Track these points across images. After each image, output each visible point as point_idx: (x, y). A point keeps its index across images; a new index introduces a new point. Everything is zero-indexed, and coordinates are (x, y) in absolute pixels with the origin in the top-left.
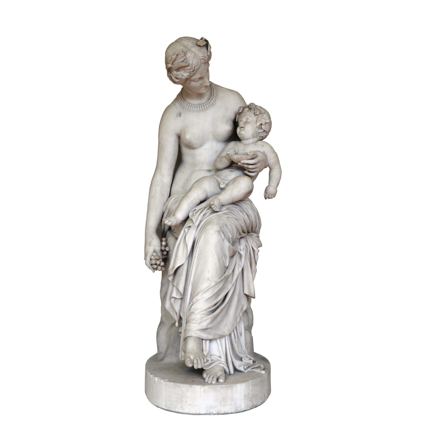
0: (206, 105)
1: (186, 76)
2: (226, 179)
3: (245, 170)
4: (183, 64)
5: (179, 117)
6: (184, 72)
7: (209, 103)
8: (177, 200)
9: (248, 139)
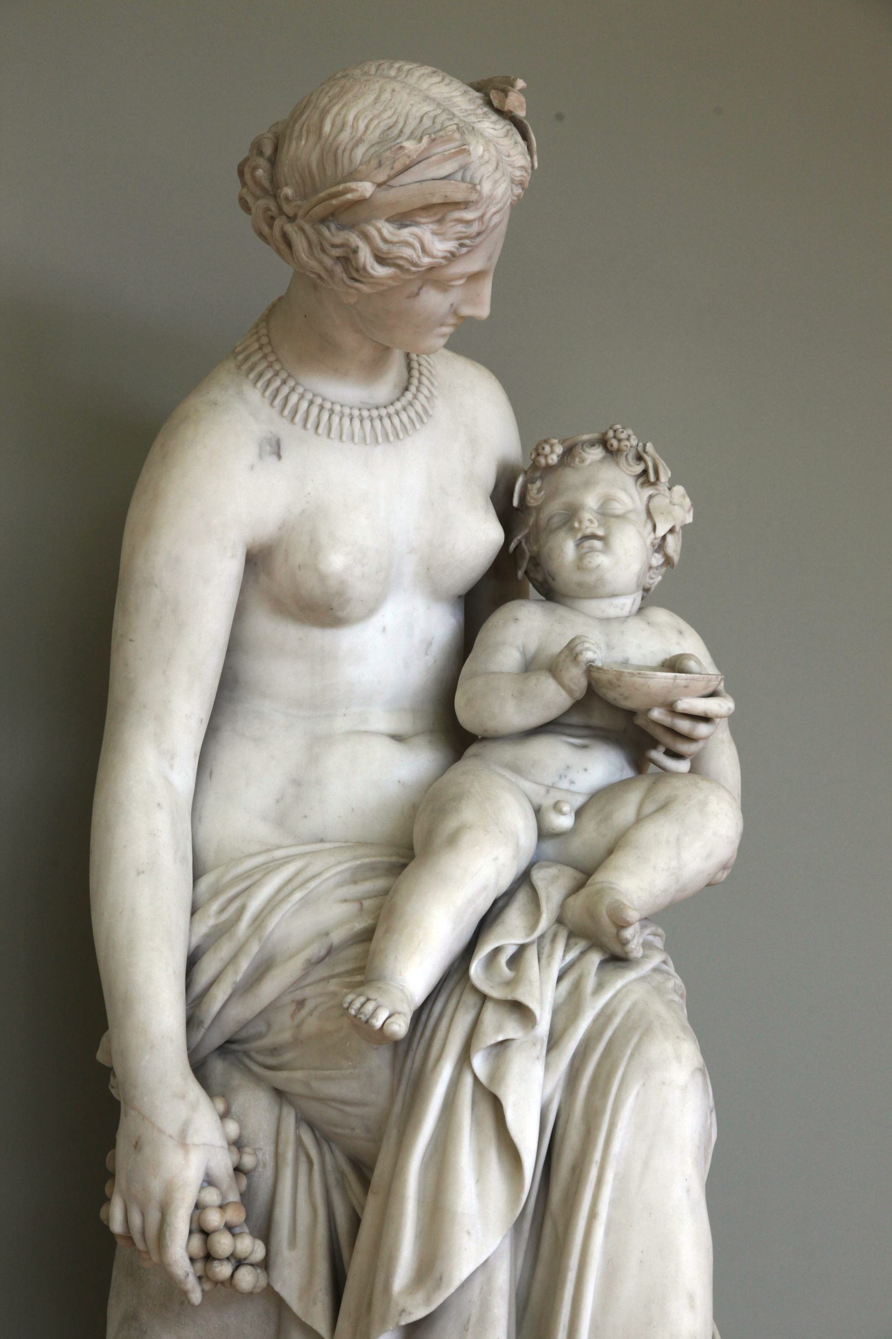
0: (397, 413)
1: (440, 254)
2: (564, 784)
3: (654, 743)
4: (456, 191)
5: (274, 458)
6: (434, 233)
7: (411, 404)
8: (311, 891)
9: (614, 595)
